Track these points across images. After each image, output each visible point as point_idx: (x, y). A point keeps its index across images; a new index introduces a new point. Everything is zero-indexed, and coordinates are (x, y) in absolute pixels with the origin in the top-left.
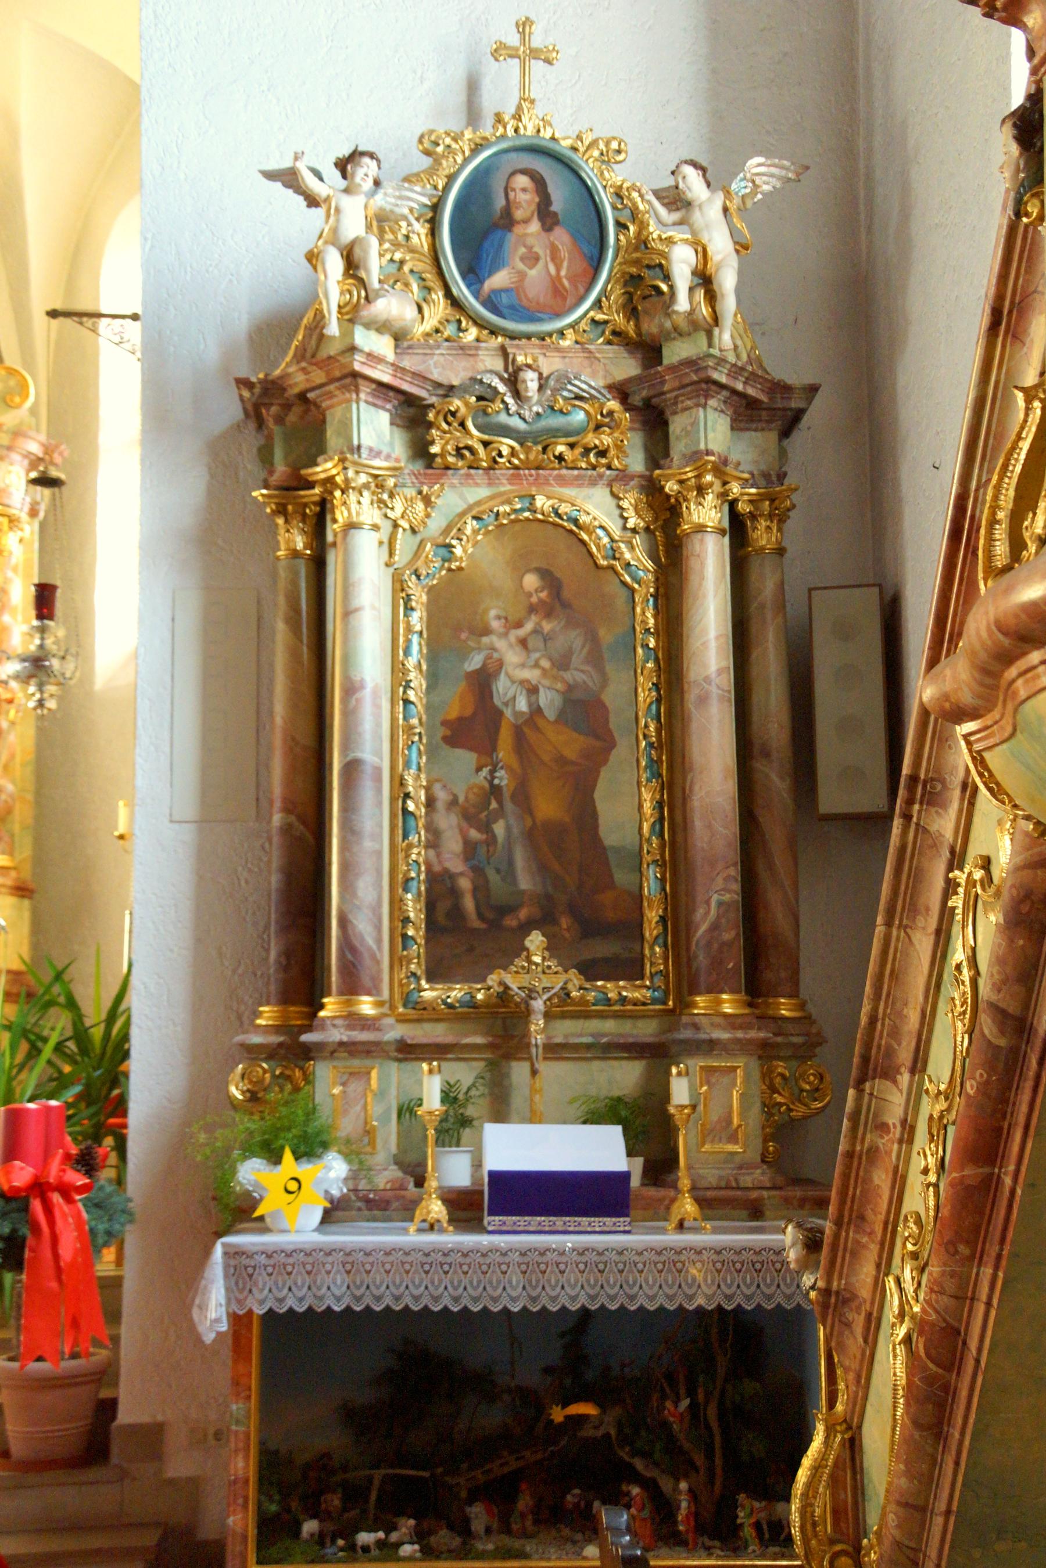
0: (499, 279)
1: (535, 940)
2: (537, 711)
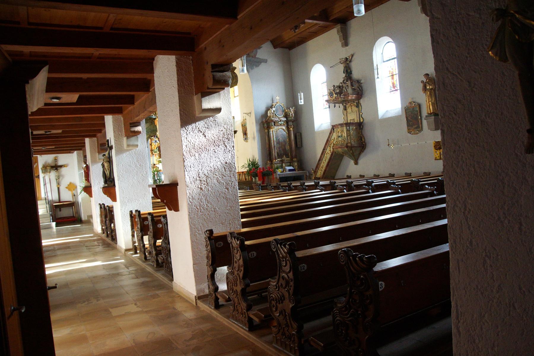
0: (278, 113)
1: (284, 156)
2: (282, 142)
